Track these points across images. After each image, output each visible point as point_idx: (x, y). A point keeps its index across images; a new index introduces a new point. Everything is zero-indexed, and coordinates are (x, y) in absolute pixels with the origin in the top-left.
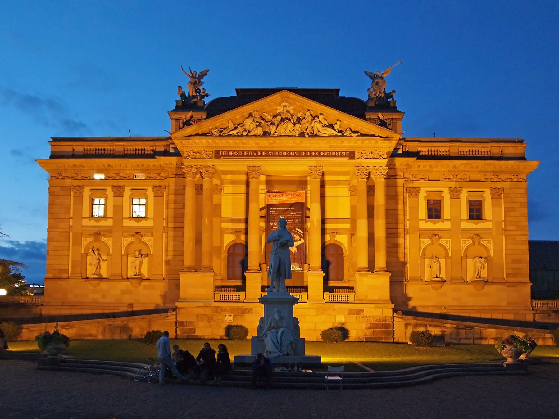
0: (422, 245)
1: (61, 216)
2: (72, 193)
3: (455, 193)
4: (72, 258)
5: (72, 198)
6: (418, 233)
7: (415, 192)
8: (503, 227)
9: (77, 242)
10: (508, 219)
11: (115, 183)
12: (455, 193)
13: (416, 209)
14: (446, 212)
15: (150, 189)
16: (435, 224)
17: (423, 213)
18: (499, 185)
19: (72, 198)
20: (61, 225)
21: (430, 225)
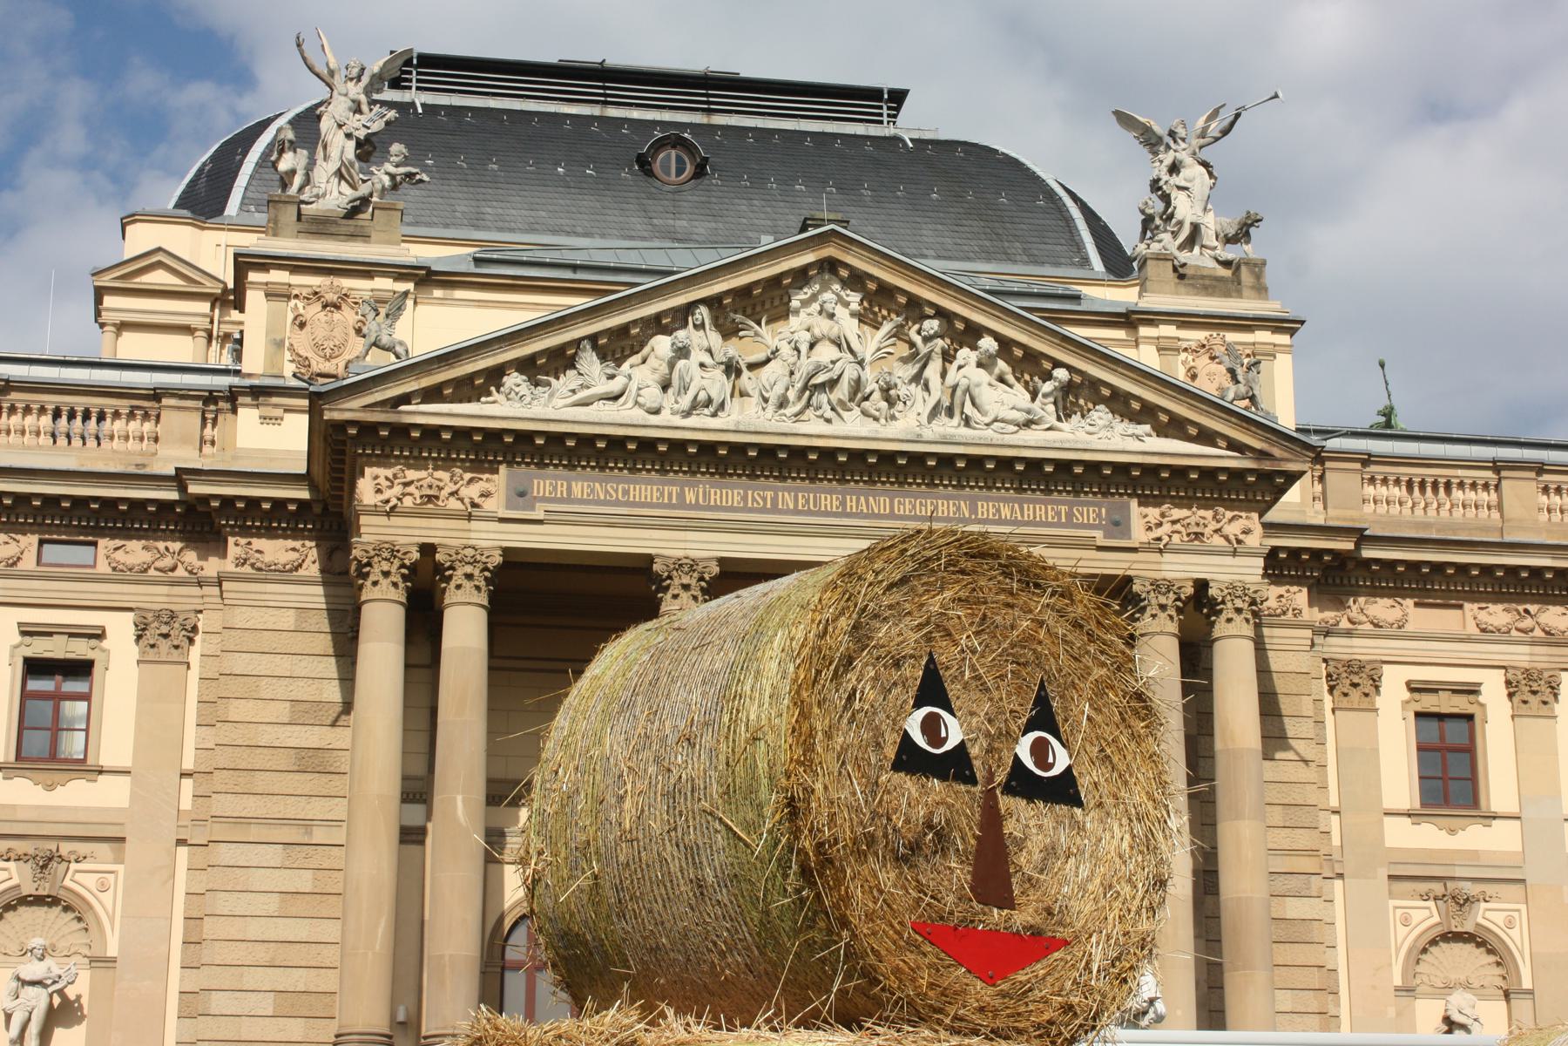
0: (1402, 931)
6: (1383, 873)
13: (1364, 757)
14: (1500, 778)
15: (120, 628)
16: (1452, 832)
17: (1399, 777)
21: (1429, 837)
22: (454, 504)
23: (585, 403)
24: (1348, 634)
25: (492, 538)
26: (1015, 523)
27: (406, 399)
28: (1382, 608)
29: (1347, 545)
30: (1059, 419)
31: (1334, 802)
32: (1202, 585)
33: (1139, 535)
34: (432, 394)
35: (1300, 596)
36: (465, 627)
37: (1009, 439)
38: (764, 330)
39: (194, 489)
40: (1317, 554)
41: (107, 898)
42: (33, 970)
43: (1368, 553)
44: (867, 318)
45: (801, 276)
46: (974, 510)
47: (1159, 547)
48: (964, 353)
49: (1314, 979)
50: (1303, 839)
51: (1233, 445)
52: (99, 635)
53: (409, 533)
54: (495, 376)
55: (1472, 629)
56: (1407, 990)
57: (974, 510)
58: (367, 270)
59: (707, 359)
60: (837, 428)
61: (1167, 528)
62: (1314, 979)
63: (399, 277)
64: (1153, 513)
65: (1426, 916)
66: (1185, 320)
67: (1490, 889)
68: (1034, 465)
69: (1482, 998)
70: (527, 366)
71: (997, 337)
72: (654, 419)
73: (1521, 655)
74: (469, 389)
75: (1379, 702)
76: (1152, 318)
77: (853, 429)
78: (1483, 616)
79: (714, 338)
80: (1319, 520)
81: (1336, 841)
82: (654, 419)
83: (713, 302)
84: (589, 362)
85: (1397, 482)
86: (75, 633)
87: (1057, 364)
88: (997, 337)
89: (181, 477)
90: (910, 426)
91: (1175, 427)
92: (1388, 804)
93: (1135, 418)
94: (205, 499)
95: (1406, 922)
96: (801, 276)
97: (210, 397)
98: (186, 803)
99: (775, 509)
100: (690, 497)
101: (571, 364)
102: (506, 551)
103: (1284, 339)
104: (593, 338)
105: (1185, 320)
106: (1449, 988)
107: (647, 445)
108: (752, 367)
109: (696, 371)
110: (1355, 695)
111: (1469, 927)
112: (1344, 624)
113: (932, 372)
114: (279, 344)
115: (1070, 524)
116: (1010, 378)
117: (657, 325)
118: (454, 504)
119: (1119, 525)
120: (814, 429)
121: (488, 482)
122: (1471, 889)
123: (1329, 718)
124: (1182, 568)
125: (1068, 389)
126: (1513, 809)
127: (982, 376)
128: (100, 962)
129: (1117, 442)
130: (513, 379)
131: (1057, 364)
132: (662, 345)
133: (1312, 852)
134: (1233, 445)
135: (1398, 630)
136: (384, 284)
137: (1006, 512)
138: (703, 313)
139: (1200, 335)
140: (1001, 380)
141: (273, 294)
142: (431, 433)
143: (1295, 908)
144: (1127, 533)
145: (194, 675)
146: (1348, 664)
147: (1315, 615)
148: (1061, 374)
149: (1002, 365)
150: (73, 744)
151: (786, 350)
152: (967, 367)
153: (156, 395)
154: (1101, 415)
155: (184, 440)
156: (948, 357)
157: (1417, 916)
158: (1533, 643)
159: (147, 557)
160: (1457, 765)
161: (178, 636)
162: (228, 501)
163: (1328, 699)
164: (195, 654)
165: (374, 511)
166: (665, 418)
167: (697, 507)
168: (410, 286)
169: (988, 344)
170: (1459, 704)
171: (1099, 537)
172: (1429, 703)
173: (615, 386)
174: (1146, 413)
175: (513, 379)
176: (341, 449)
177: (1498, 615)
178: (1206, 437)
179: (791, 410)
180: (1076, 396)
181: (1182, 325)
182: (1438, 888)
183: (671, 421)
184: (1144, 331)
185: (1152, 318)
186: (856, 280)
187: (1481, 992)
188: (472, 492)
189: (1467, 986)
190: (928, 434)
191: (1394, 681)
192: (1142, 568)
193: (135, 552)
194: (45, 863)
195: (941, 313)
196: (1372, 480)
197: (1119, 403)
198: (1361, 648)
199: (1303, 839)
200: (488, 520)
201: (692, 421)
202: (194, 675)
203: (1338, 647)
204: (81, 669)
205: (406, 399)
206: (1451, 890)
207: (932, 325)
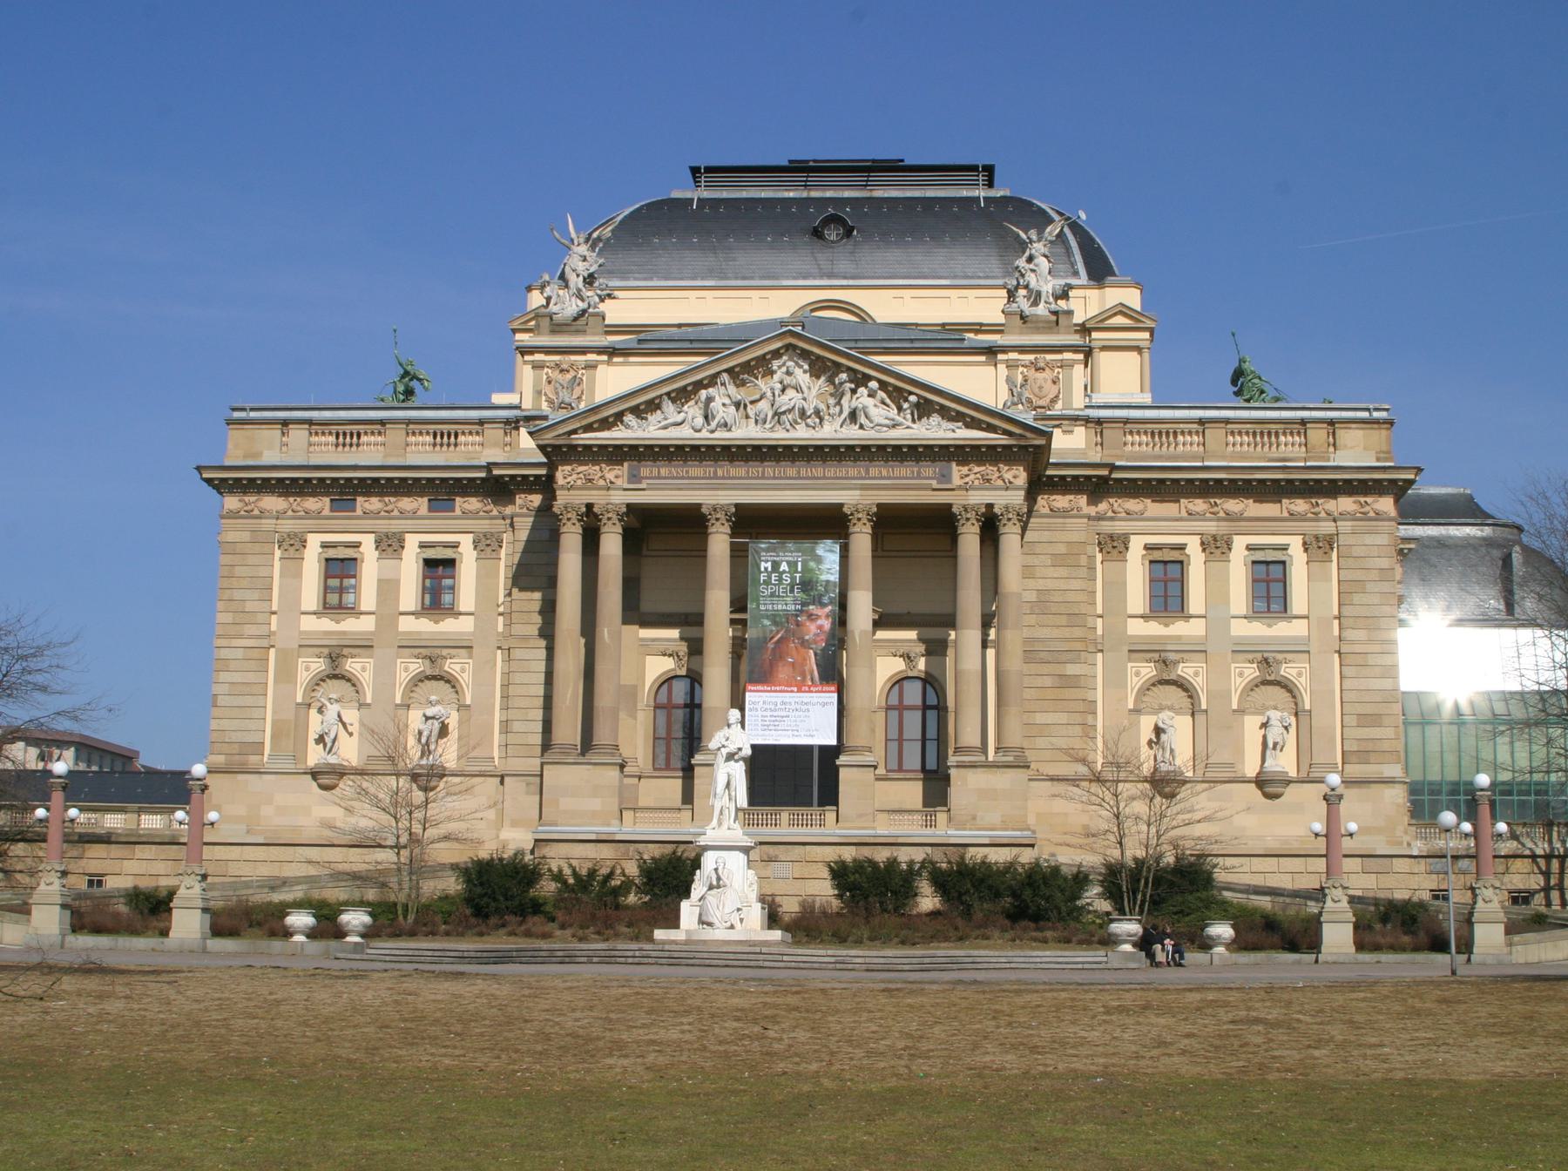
1: (249, 607)
2: (278, 553)
3: (1216, 547)
4: (274, 712)
5: (277, 564)
6: (1126, 648)
7: (1114, 545)
8: (1336, 633)
9: (286, 674)
10: (1347, 611)
11: (383, 525)
12: (1216, 547)
13: (1117, 588)
16: (1166, 625)
18: (1327, 528)
19: (277, 564)
20: (250, 630)
21: (1154, 629)
22: (602, 482)
23: (665, 428)
24: (1112, 519)
25: (620, 498)
26: (889, 478)
27: (574, 432)
28: (1132, 504)
29: (1105, 472)
30: (914, 421)
31: (1099, 611)
32: (990, 506)
33: (956, 481)
34: (588, 428)
35: (1082, 500)
36: (612, 545)
37: (883, 435)
38: (760, 382)
39: (496, 472)
40: (1088, 478)
41: (465, 675)
42: (430, 712)
43: (1115, 475)
44: (815, 373)
45: (776, 354)
46: (867, 472)
47: (966, 488)
48: (862, 390)
49: (1081, 706)
50: (1078, 632)
51: (1005, 432)
52: (455, 546)
53: (580, 498)
54: (619, 416)
55: (1184, 514)
56: (1137, 711)
57: (867, 472)
58: (583, 351)
59: (727, 401)
60: (792, 434)
61: (972, 477)
62: (1081, 706)
63: (599, 353)
64: (965, 470)
65: (1148, 671)
66: (1022, 349)
67: (1185, 656)
68: (898, 448)
69: (1178, 713)
70: (637, 411)
71: (879, 381)
72: (698, 435)
73: (1211, 527)
74: (605, 424)
75: (1129, 555)
76: (1005, 349)
77: (802, 434)
78: (1190, 506)
79: (732, 389)
80: (1098, 460)
81: (1099, 632)
82: (698, 435)
83: (729, 371)
84: (669, 407)
85: (1146, 433)
86: (447, 545)
87: (911, 393)
88: (879, 381)
89: (489, 466)
90: (832, 431)
91: (973, 424)
92: (1130, 611)
93: (951, 419)
94: (502, 476)
95: (1137, 674)
96: (776, 354)
97: (507, 422)
98: (500, 629)
99: (763, 477)
100: (720, 473)
101: (658, 407)
102: (628, 505)
103: (1081, 356)
104: (668, 394)
105: (1022, 349)
106: (1161, 709)
107: (695, 448)
108: (752, 402)
109: (721, 408)
110: (1115, 552)
111: (1173, 677)
112: (1110, 514)
113: (845, 401)
114: (539, 393)
115: (919, 477)
116: (888, 401)
117: (699, 385)
118: (602, 482)
119: (945, 477)
120: (780, 436)
121: (617, 470)
122: (1172, 656)
123: (1099, 566)
124: (978, 498)
125: (917, 405)
126: (1203, 612)
127: (870, 402)
128: (462, 707)
129: (941, 434)
130: (629, 418)
131: (911, 393)
132: (703, 394)
133: (1083, 640)
134: (1005, 432)
135: (1140, 516)
136: (592, 357)
137: (884, 473)
138: (725, 376)
139: (1031, 357)
140: (883, 403)
141: (537, 366)
142: (588, 448)
143: (1071, 669)
144: (950, 481)
145: (502, 564)
146: (1111, 537)
147: (1092, 511)
148: (913, 398)
149: (881, 394)
150: (446, 598)
151: (769, 394)
152: (863, 399)
153: (481, 422)
154: (935, 419)
155: (495, 445)
156: (854, 391)
157: (1144, 671)
158: (1219, 520)
159: (479, 505)
160: (1173, 589)
161: (495, 545)
162: (513, 477)
163: (1099, 557)
164: (503, 552)
165: (562, 487)
166: (705, 434)
167: (723, 478)
168: (605, 358)
169: (873, 385)
170: (1175, 555)
171: (934, 483)
172: (1157, 555)
173: (680, 418)
174: (958, 417)
175: (629, 418)
176: (557, 454)
177: (1199, 505)
178: (991, 428)
179: (768, 426)
180: (924, 409)
181: (1021, 352)
182: (1156, 656)
183: (705, 436)
184: (1000, 357)
185: (1005, 349)
186: (805, 354)
187: (1178, 712)
188: (610, 476)
189: (1171, 708)
190: (840, 435)
191: (1137, 545)
192: (956, 500)
193: (473, 503)
194: (432, 660)
195: (849, 369)
196: (1131, 433)
197: (945, 413)
198: (1119, 527)
199: (1078, 632)
200: (616, 491)
201: (717, 435)
202: (502, 564)
203: (1107, 527)
204: (450, 563)
205: (574, 432)
206: (1162, 656)
207: (844, 376)
